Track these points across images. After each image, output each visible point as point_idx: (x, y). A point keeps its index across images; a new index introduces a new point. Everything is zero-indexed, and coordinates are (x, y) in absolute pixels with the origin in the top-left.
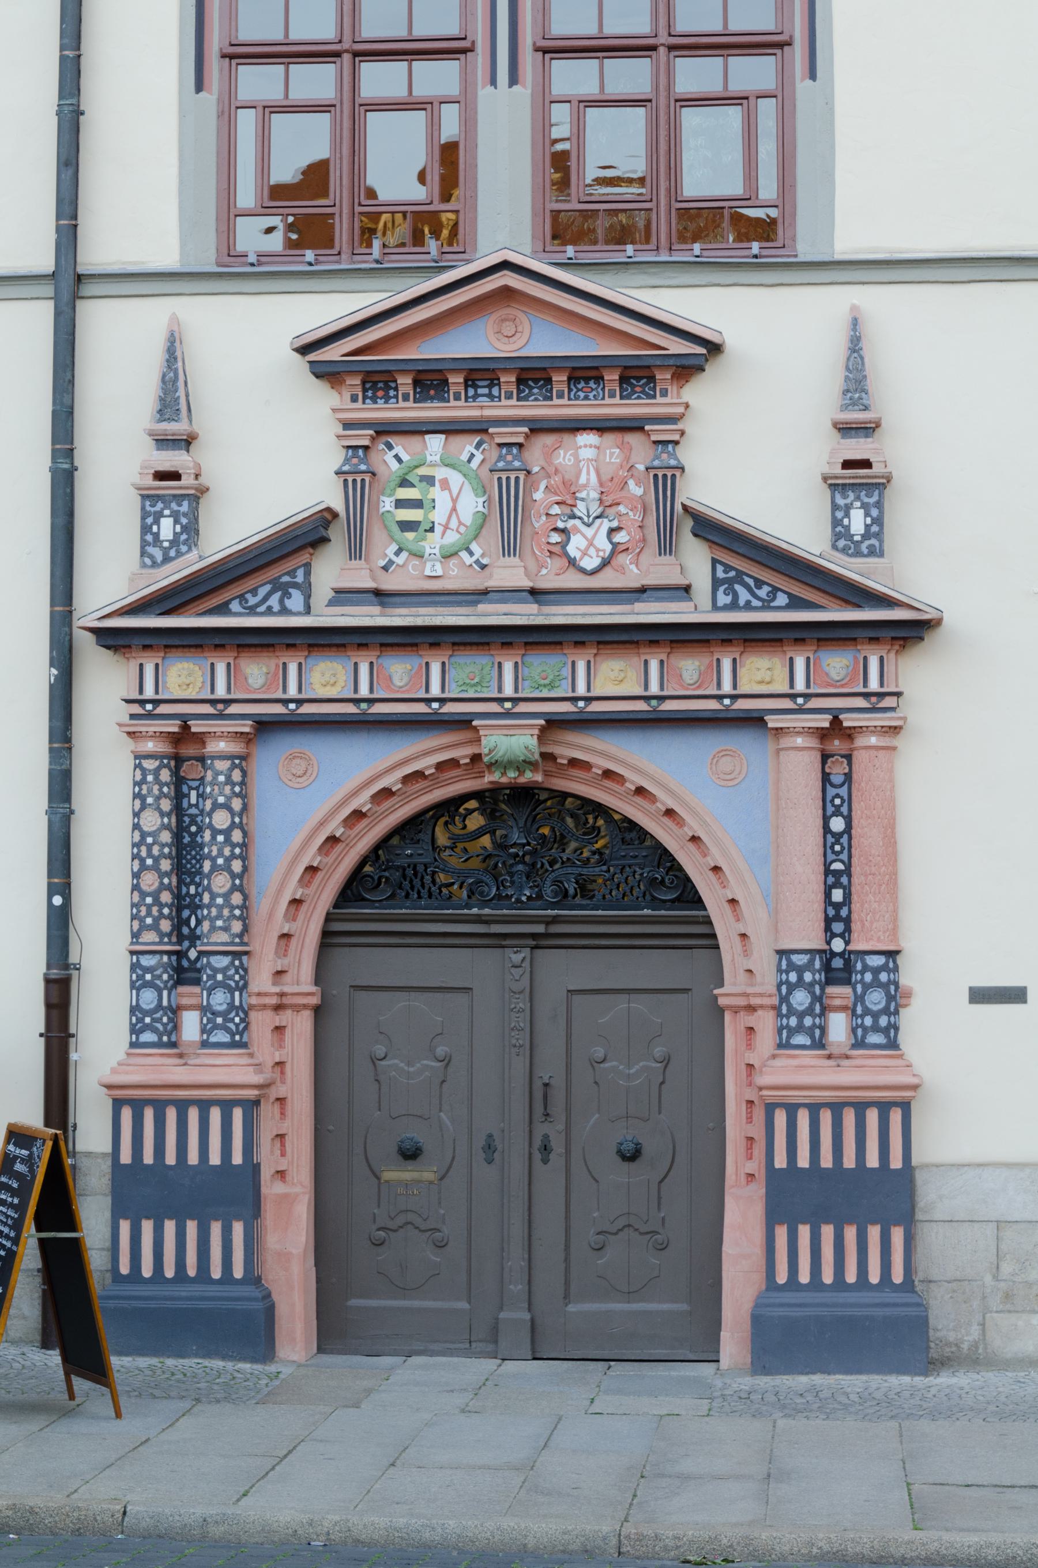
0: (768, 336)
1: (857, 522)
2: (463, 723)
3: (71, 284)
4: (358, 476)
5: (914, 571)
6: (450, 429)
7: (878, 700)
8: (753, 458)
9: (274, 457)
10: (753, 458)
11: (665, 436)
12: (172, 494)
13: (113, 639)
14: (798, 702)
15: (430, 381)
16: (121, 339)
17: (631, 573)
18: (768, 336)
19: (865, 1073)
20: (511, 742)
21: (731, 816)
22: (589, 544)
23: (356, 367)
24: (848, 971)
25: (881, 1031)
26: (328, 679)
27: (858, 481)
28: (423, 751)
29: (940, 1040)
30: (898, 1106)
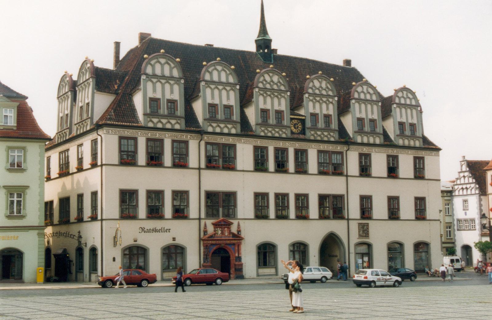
0: (235, 222)
1: (240, 233)
2: (221, 244)
3: (200, 219)
4: (215, 231)
6: (220, 228)
7: (241, 243)
8: (234, 229)
9: (211, 229)
11: (229, 229)
13: (204, 240)
14: (237, 243)
15: (219, 225)
16: (203, 222)
17: (228, 236)
18: (235, 222)
19: (240, 263)
20: (223, 245)
22: (226, 234)
27: (239, 231)
28: (219, 246)
30: (242, 265)
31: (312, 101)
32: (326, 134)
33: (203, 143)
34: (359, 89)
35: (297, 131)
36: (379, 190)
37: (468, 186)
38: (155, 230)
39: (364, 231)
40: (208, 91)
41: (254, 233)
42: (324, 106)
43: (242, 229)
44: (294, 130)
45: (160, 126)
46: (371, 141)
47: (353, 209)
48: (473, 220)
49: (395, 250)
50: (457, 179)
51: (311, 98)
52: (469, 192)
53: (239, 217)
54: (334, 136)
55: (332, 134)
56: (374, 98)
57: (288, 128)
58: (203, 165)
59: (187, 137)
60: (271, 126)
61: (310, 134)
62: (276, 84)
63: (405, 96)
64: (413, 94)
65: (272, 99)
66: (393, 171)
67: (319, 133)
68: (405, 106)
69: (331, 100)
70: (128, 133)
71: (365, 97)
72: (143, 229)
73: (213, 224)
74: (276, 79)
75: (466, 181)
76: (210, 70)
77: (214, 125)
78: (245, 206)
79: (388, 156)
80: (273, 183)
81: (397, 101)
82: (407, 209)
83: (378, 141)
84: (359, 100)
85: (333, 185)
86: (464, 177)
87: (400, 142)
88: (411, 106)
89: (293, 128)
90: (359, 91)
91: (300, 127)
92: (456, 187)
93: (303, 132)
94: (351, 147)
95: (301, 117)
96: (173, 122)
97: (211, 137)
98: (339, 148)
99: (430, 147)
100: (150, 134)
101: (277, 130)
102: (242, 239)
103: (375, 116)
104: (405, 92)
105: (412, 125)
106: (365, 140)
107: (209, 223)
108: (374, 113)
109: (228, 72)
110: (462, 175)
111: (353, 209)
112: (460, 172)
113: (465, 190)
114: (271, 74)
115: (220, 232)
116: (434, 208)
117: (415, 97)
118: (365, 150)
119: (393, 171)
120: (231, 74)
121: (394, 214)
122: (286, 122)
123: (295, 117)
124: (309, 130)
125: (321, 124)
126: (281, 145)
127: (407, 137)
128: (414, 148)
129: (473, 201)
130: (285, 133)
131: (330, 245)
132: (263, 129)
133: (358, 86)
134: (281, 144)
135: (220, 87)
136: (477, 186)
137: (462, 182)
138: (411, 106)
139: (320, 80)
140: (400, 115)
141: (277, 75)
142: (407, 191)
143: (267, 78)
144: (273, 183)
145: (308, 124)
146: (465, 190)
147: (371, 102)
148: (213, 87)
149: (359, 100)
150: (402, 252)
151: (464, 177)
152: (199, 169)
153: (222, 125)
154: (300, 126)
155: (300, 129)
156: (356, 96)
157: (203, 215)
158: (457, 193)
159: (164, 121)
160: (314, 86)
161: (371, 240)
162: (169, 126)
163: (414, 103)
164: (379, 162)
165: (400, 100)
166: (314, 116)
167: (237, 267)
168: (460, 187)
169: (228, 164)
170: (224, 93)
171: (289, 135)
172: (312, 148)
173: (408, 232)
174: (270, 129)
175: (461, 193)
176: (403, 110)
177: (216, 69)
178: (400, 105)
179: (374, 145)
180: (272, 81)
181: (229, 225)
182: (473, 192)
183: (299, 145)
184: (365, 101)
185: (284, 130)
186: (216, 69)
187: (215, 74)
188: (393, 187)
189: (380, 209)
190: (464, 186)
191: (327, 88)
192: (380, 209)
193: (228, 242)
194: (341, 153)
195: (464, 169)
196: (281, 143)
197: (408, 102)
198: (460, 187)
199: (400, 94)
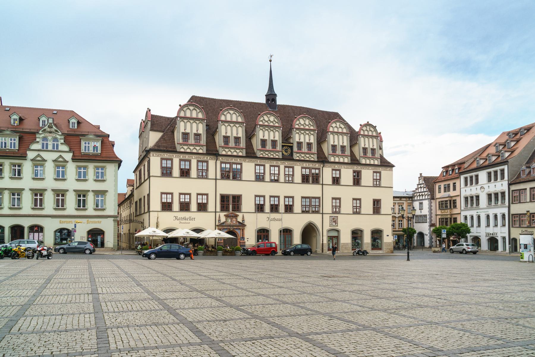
0: (240, 215)
3: (216, 212)
5: (245, 223)
8: (240, 219)
9: (223, 219)
10: (240, 219)
11: (236, 219)
12: (219, 220)
16: (218, 214)
21: (239, 232)
23: (226, 216)
24: (243, 238)
25: (244, 240)
26: (225, 227)
27: (243, 220)
29: (246, 240)
31: (298, 133)
32: (308, 156)
33: (218, 163)
34: (334, 125)
36: (347, 193)
37: (423, 194)
38: (185, 219)
39: (334, 221)
40: (223, 128)
41: (252, 222)
42: (307, 136)
43: (245, 219)
44: (285, 153)
45: (188, 151)
46: (341, 160)
47: (327, 207)
48: (425, 216)
49: (356, 234)
50: (416, 189)
51: (298, 131)
52: (424, 198)
53: (243, 211)
54: (315, 158)
55: (312, 156)
56: (345, 131)
58: (219, 177)
59: (207, 158)
61: (296, 156)
62: (272, 122)
63: (368, 130)
64: (375, 127)
65: (269, 132)
66: (357, 181)
67: (303, 155)
68: (368, 136)
69: (312, 133)
70: (166, 155)
71: (368, 133)
72: (176, 218)
73: (225, 215)
74: (272, 118)
75: (422, 191)
76: (225, 113)
77: (227, 150)
78: (248, 205)
79: (354, 172)
80: (267, 189)
81: (362, 133)
82: (367, 207)
83: (346, 160)
84: (333, 133)
85: (312, 190)
86: (421, 187)
87: (363, 161)
88: (372, 137)
89: (284, 152)
90: (334, 126)
91: (289, 151)
92: (415, 194)
93: (292, 154)
94: (325, 164)
96: (198, 148)
97: (224, 158)
98: (317, 165)
99: (386, 165)
100: (182, 156)
101: (272, 153)
102: (245, 226)
103: (345, 144)
104: (368, 127)
105: (373, 150)
106: (337, 160)
107: (222, 214)
108: (345, 141)
109: (238, 115)
110: (419, 186)
111: (327, 207)
112: (418, 185)
113: (421, 197)
114: (269, 116)
115: (230, 221)
116: (387, 206)
117: (376, 130)
118: (337, 167)
119: (357, 181)
120: (239, 116)
121: (357, 211)
122: (279, 148)
125: (305, 149)
127: (369, 158)
128: (374, 165)
129: (426, 203)
131: (309, 231)
132: (262, 152)
133: (333, 123)
134: (275, 163)
135: (232, 125)
136: (429, 193)
137: (420, 191)
138: (372, 137)
140: (363, 142)
142: (367, 194)
143: (266, 119)
144: (267, 189)
145: (295, 149)
146: (421, 197)
147: (342, 133)
148: (226, 124)
149: (333, 133)
150: (361, 237)
151: (421, 187)
152: (216, 179)
153: (232, 150)
156: (331, 129)
157: (218, 209)
158: (416, 198)
159: (192, 148)
160: (300, 123)
161: (339, 228)
162: (195, 151)
163: (374, 134)
164: (347, 175)
165: (364, 133)
166: (300, 144)
167: (242, 244)
168: (418, 194)
169: (236, 175)
170: (234, 128)
171: (281, 157)
173: (367, 223)
174: (267, 153)
175: (418, 198)
176: (371, 139)
177: (229, 113)
178: (364, 136)
179: (344, 163)
180: (269, 120)
181: (236, 216)
182: (426, 197)
183: (287, 163)
184: (337, 133)
186: (229, 113)
187: (228, 116)
188: (357, 192)
189: (347, 207)
190: (421, 194)
191: (310, 124)
192: (347, 207)
193: (235, 227)
194: (319, 169)
195: (421, 183)
197: (370, 133)
198: (418, 194)
199: (364, 128)
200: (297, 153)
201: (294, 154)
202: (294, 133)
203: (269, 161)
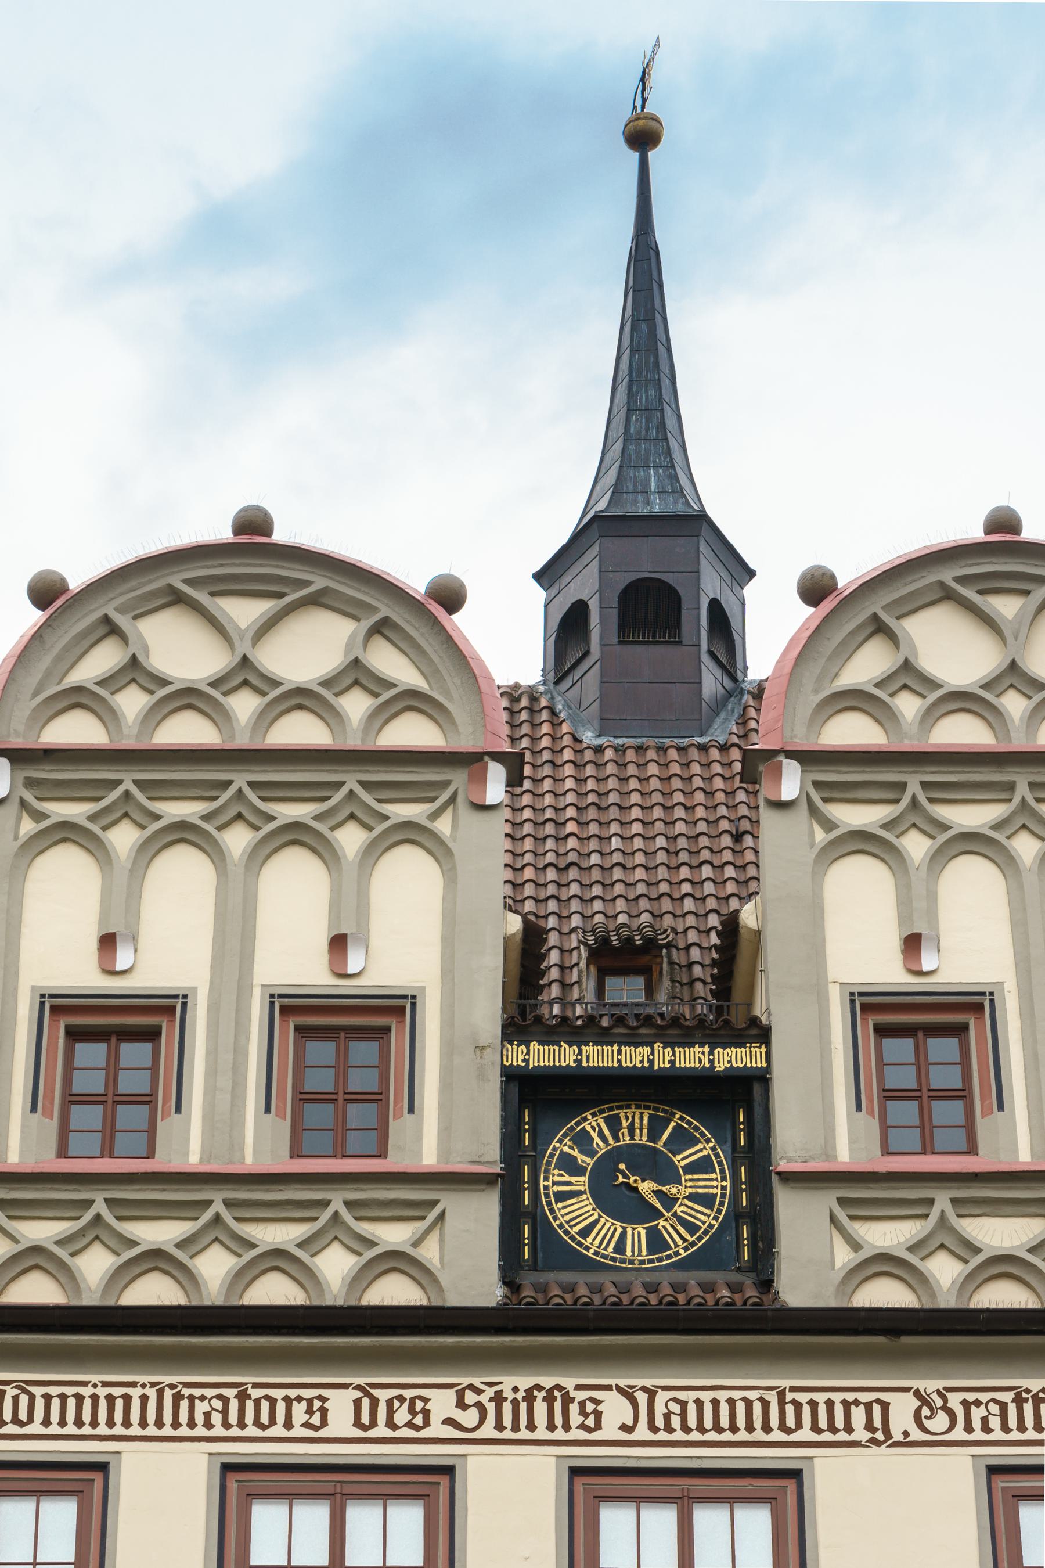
35: (656, 1242)
57: (450, 1201)
60: (182, 1189)
93: (753, 1224)
95: (692, 1058)
123: (599, 1057)
124: (826, 1200)
126: (340, 1422)
130: (396, 1261)
134: (337, 1413)
139: (1006, 607)
141: (317, 600)
154: (715, 1183)
155: (707, 1219)
172: (882, 1435)
185: (394, 1235)
196: (341, 1405)
200: (858, 1190)
201: (798, 1217)
202: (783, 843)
203: (209, 1386)
